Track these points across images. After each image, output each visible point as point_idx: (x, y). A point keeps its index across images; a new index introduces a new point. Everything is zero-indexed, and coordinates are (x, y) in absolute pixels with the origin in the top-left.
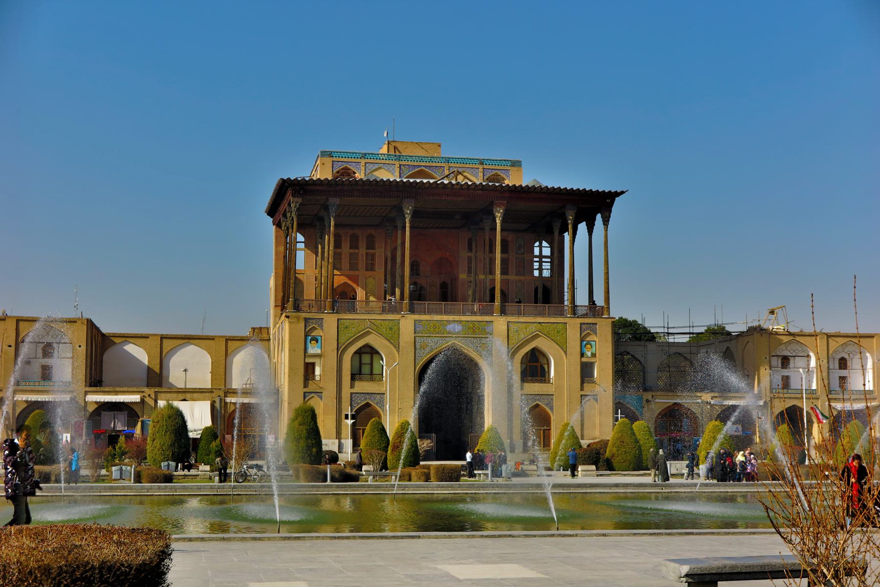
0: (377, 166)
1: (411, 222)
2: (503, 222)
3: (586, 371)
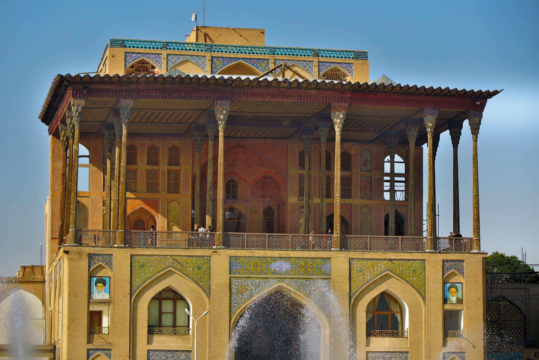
0: (182, 59)
1: (225, 131)
2: (344, 130)
3: (450, 322)
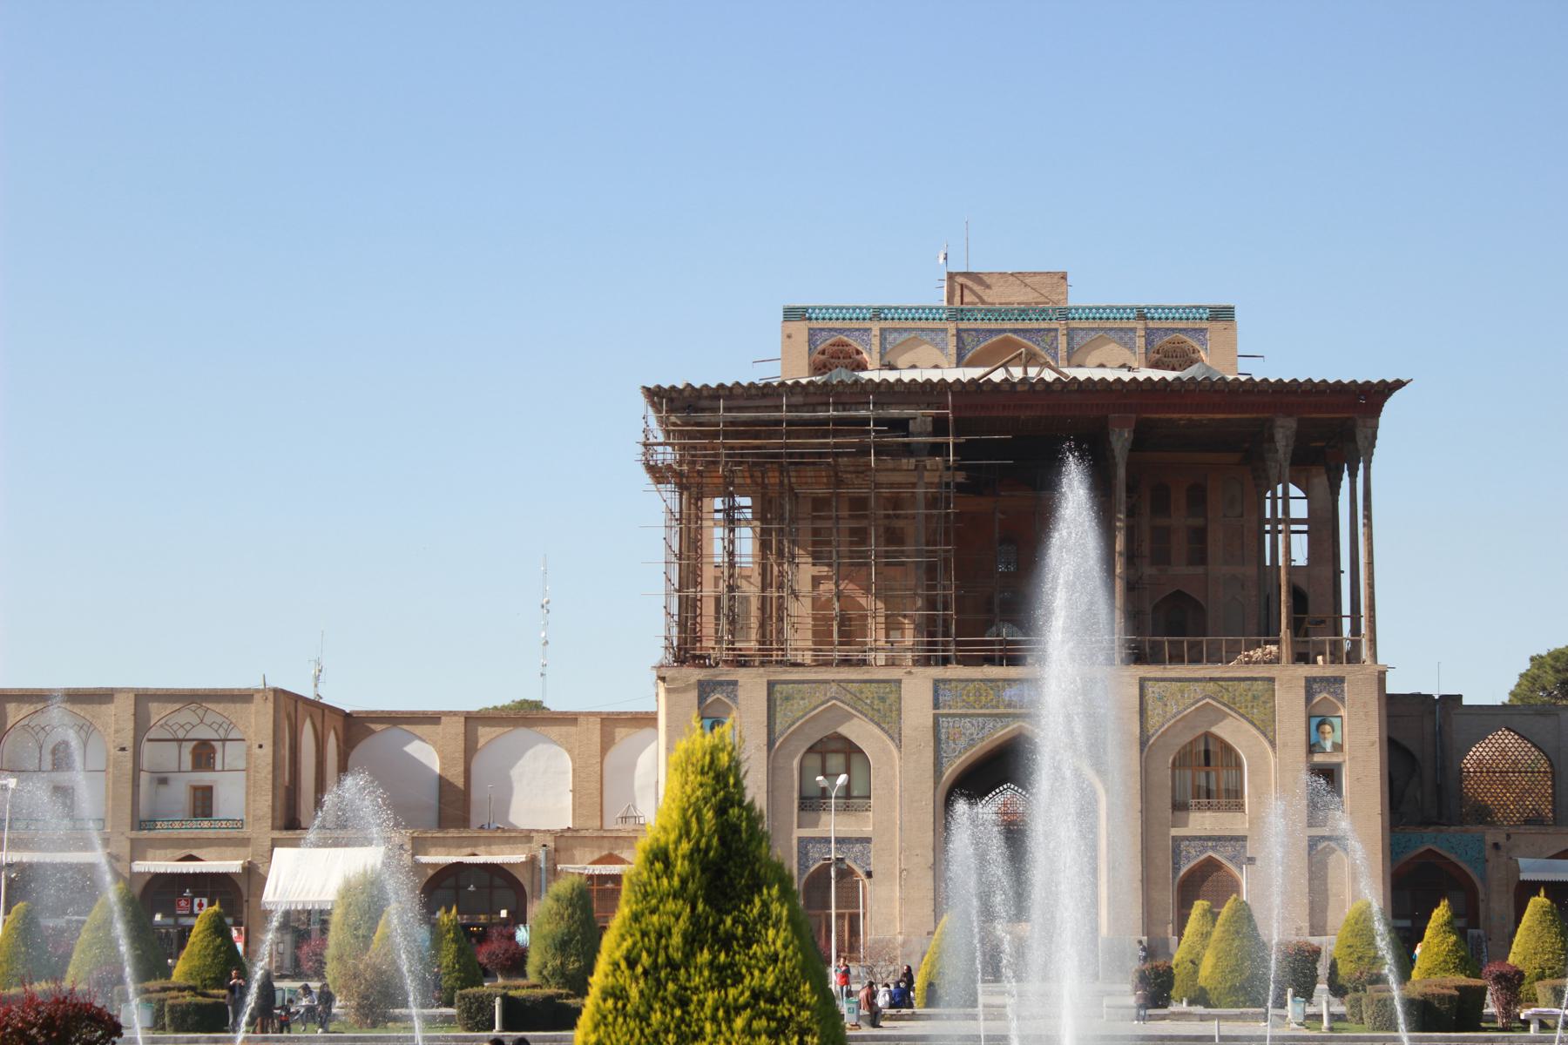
0: (906, 336)
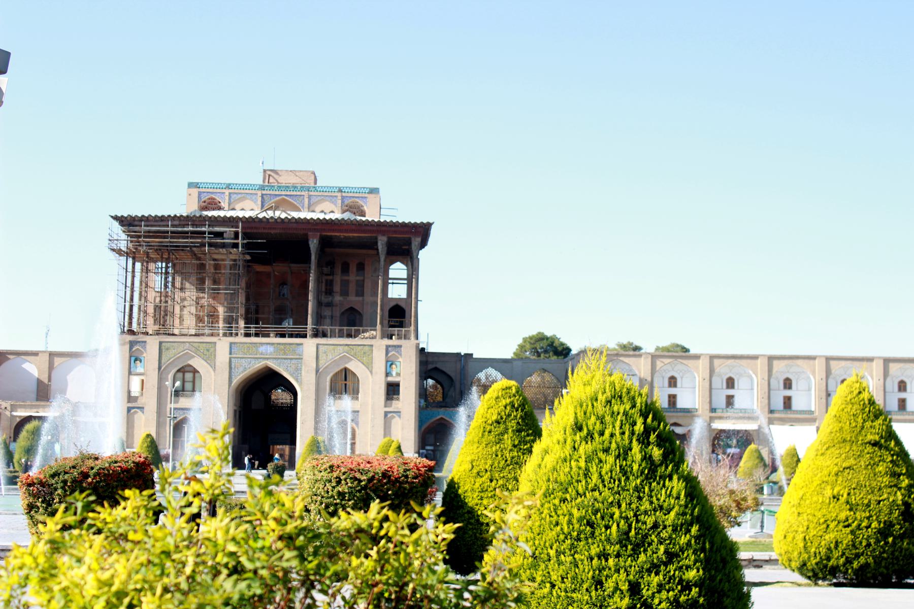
0: (240, 196)
3: (392, 390)
